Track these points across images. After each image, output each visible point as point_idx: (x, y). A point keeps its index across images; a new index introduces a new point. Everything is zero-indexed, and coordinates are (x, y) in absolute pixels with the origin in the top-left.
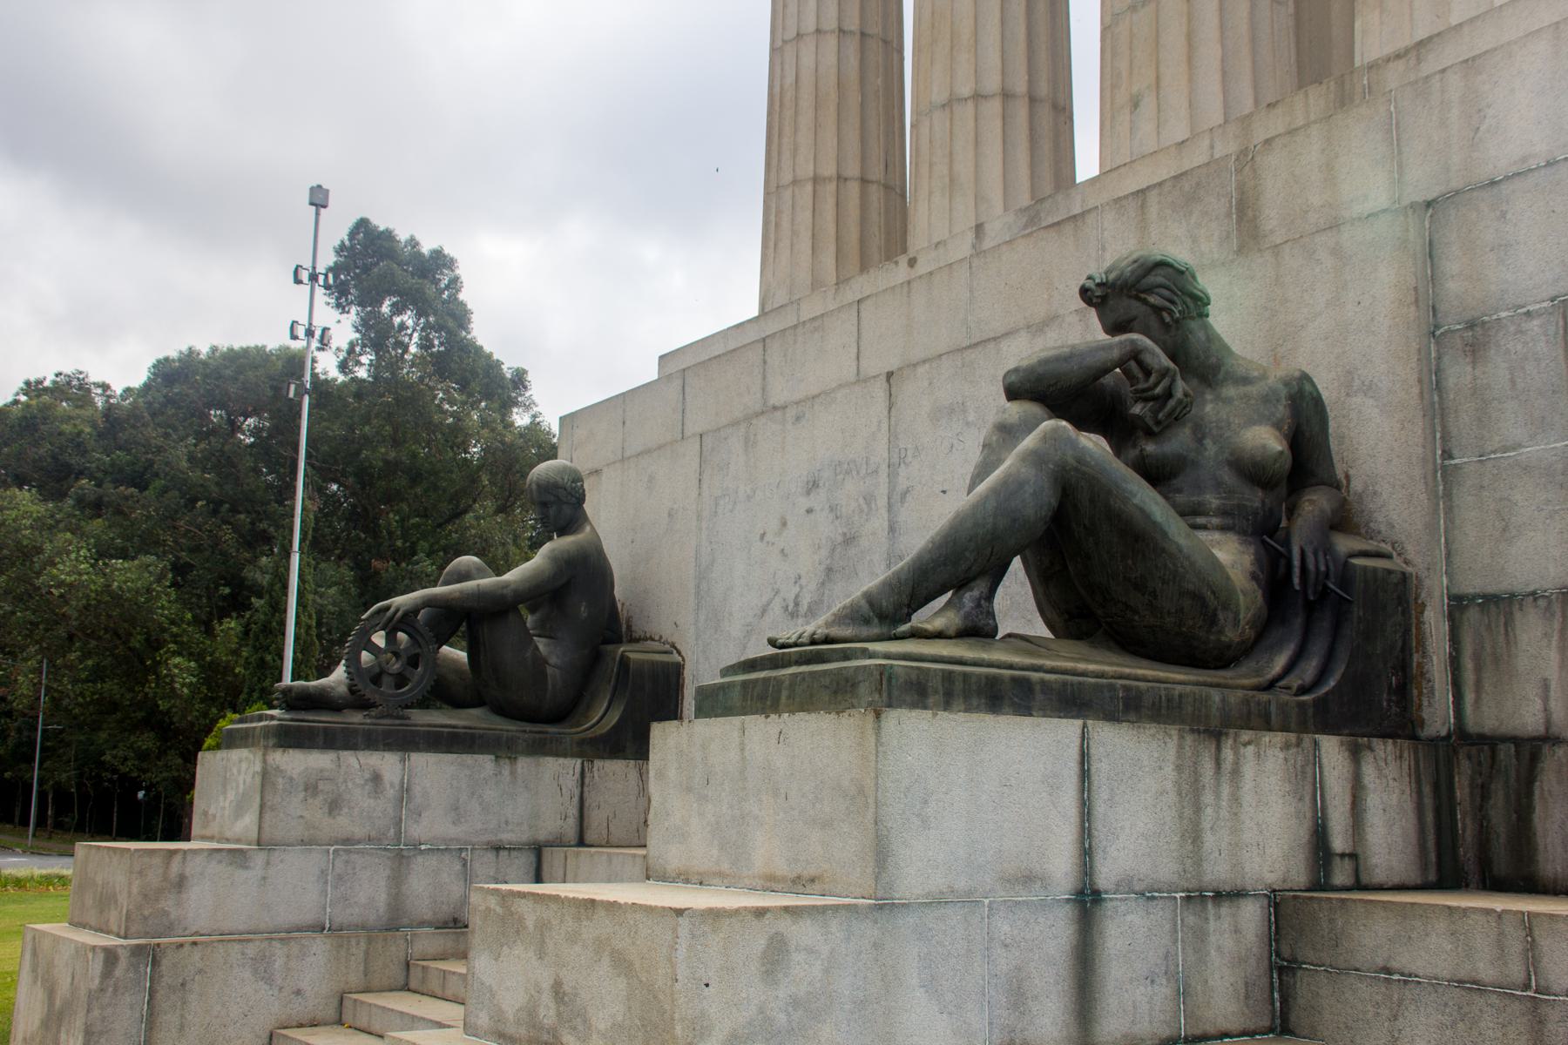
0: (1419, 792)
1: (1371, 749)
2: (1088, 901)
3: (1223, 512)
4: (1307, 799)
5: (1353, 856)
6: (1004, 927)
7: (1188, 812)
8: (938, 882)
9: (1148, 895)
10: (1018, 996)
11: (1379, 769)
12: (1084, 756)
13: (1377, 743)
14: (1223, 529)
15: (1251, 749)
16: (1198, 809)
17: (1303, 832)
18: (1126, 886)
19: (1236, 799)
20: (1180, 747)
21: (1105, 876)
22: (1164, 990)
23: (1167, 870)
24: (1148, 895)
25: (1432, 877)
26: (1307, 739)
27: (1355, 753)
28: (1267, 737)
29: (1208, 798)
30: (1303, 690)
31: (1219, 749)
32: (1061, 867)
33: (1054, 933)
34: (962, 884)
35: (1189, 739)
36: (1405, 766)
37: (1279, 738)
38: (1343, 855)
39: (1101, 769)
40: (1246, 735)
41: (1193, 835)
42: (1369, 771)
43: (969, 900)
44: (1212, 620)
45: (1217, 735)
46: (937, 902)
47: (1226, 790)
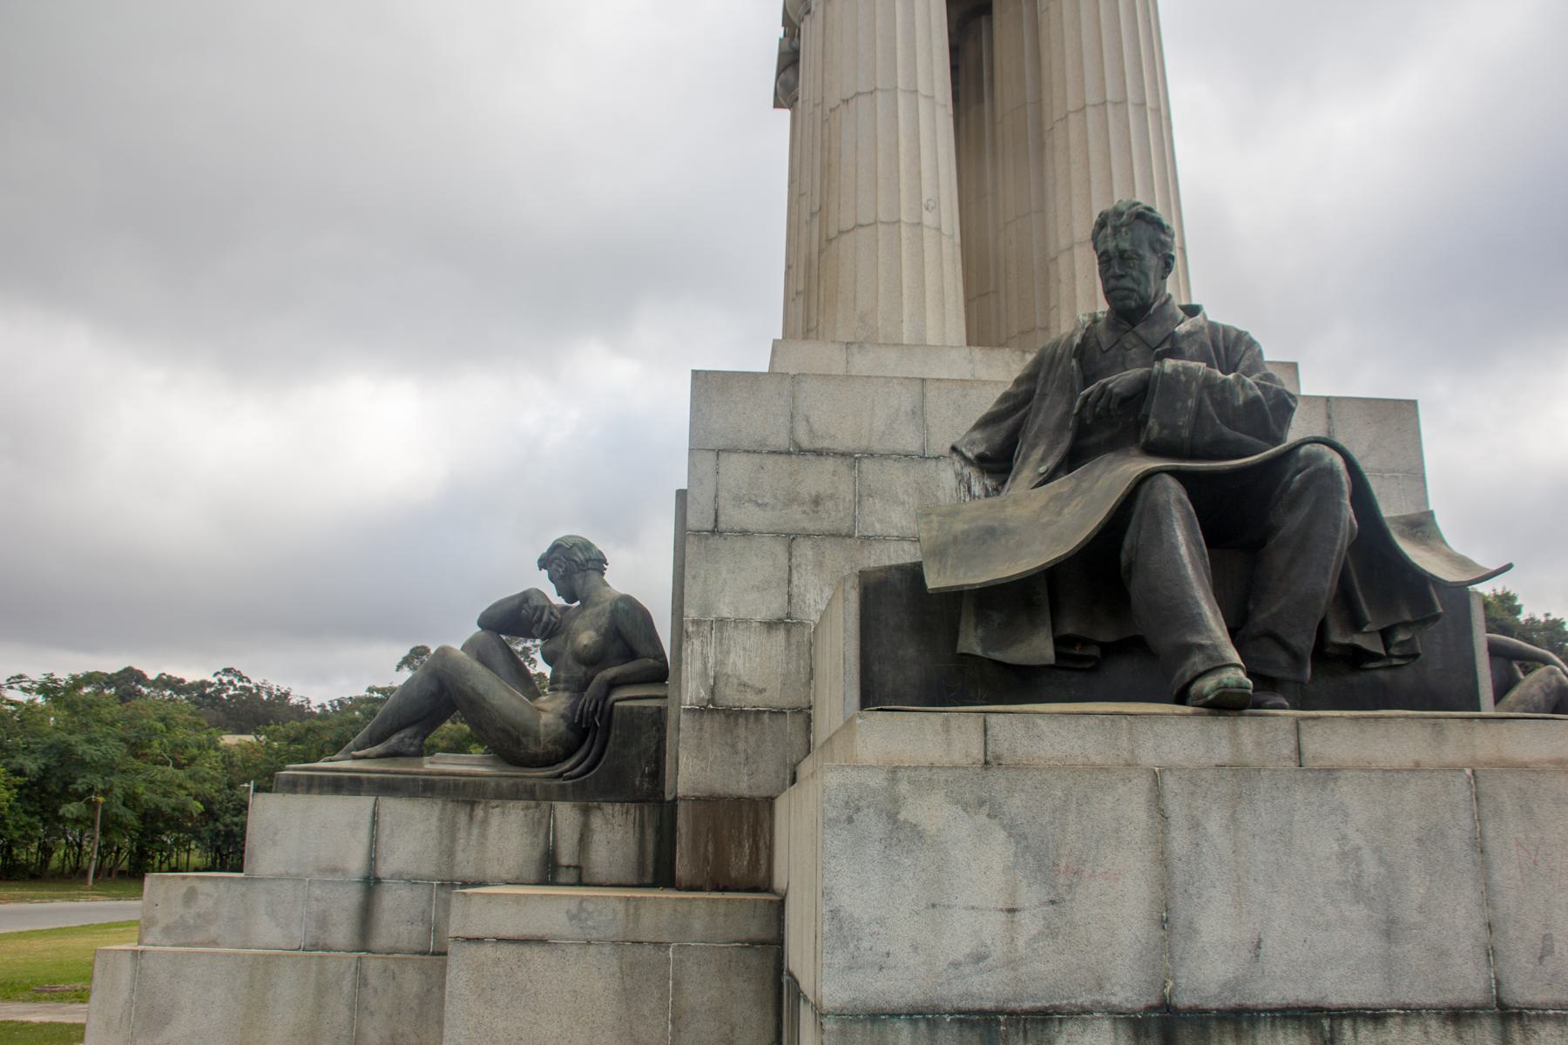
0: (642, 833)
1: (599, 808)
2: (372, 883)
3: (566, 681)
4: (542, 836)
5: (578, 868)
6: (317, 892)
7: (446, 841)
8: (280, 869)
9: (413, 881)
10: (323, 922)
11: (607, 822)
12: (375, 814)
13: (608, 808)
14: (565, 690)
15: (497, 810)
16: (453, 840)
17: (537, 854)
18: (398, 876)
19: (483, 836)
20: (443, 809)
21: (384, 870)
22: (420, 928)
23: (428, 868)
24: (413, 881)
25: (648, 880)
26: (545, 805)
27: (586, 812)
28: (511, 804)
29: (462, 834)
30: (570, 778)
31: (472, 810)
32: (356, 864)
33: (351, 897)
34: (293, 871)
35: (450, 805)
36: (631, 818)
37: (521, 804)
38: (568, 867)
39: (386, 820)
40: (494, 803)
41: (450, 853)
42: (597, 821)
43: (297, 879)
44: (518, 742)
45: (472, 804)
46: (278, 878)
47: (475, 831)
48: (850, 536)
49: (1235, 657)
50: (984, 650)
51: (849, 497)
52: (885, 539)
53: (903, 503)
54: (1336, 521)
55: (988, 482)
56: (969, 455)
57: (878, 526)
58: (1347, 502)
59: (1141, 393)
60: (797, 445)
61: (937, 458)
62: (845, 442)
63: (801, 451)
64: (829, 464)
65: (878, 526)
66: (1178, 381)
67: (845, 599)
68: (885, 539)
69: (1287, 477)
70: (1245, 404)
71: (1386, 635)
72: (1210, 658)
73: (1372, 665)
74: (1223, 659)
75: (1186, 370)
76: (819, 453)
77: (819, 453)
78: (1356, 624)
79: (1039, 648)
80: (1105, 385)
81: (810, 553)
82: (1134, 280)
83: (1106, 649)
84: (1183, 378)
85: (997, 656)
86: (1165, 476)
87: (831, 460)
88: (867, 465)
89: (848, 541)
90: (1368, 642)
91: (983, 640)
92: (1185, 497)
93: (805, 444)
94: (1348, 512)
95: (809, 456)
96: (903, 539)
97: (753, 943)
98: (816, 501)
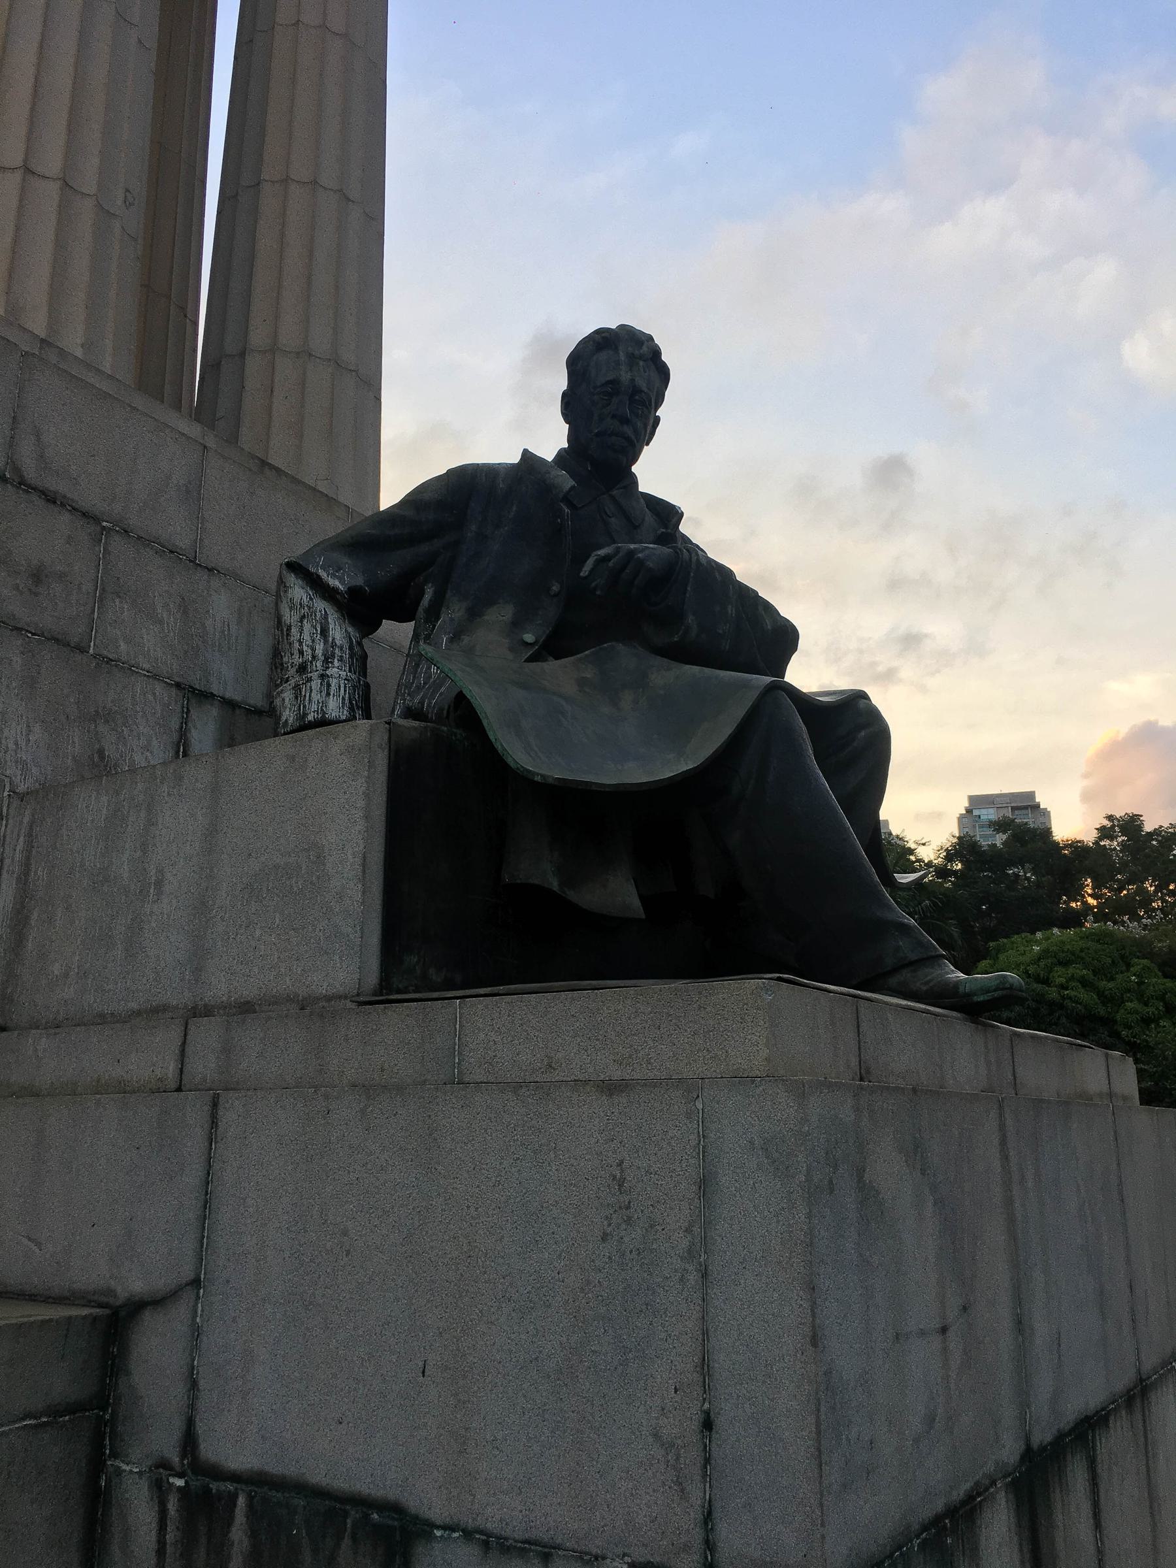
48: (83, 650)
51: (88, 587)
53: (161, 622)
55: (350, 629)
57: (123, 646)
60: (17, 470)
61: (210, 570)
62: (90, 497)
63: (22, 484)
64: (64, 520)
65: (123, 646)
67: (371, 764)
68: (130, 669)
76: (51, 498)
77: (51, 498)
79: (618, 893)
80: (631, 553)
81: (18, 661)
82: (636, 431)
87: (66, 517)
88: (118, 543)
89: (78, 657)
93: (31, 472)
95: (34, 497)
96: (155, 677)
97: (55, 1412)
98: (38, 576)
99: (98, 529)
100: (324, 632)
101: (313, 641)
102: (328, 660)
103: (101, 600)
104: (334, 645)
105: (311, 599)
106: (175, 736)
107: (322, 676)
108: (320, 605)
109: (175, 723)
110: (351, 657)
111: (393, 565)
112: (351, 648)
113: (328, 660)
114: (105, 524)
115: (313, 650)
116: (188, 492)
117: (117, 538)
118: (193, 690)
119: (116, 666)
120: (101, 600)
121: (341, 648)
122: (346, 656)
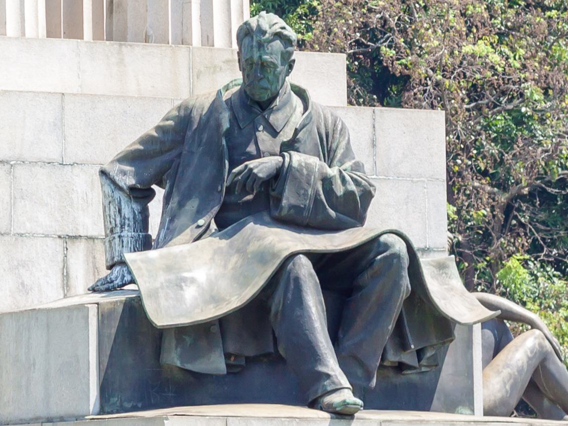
48: (8, 234)
49: (344, 381)
50: (181, 363)
52: (33, 235)
54: (397, 284)
56: (122, 184)
57: (28, 225)
58: (405, 273)
59: (279, 176)
65: (28, 225)
66: (302, 174)
68: (33, 235)
69: (371, 256)
70: (344, 194)
71: (420, 353)
72: (334, 383)
73: (409, 372)
74: (341, 384)
75: (308, 166)
78: (402, 344)
83: (248, 359)
84: (305, 172)
85: (189, 367)
86: (301, 256)
89: (6, 238)
90: (408, 358)
91: (181, 357)
92: (318, 281)
94: (406, 282)
96: (47, 236)
99: (9, 166)
100: (120, 211)
101: (115, 216)
102: (122, 226)
103: (14, 204)
104: (124, 218)
105: (113, 192)
106: (61, 265)
107: (120, 237)
108: (117, 194)
109: (60, 257)
110: (135, 223)
111: (158, 162)
112: (134, 218)
113: (122, 226)
114: (12, 163)
115: (115, 221)
116: (55, 125)
117: (19, 167)
118: (70, 237)
119: (26, 236)
120: (14, 204)
121: (129, 219)
122: (132, 223)
